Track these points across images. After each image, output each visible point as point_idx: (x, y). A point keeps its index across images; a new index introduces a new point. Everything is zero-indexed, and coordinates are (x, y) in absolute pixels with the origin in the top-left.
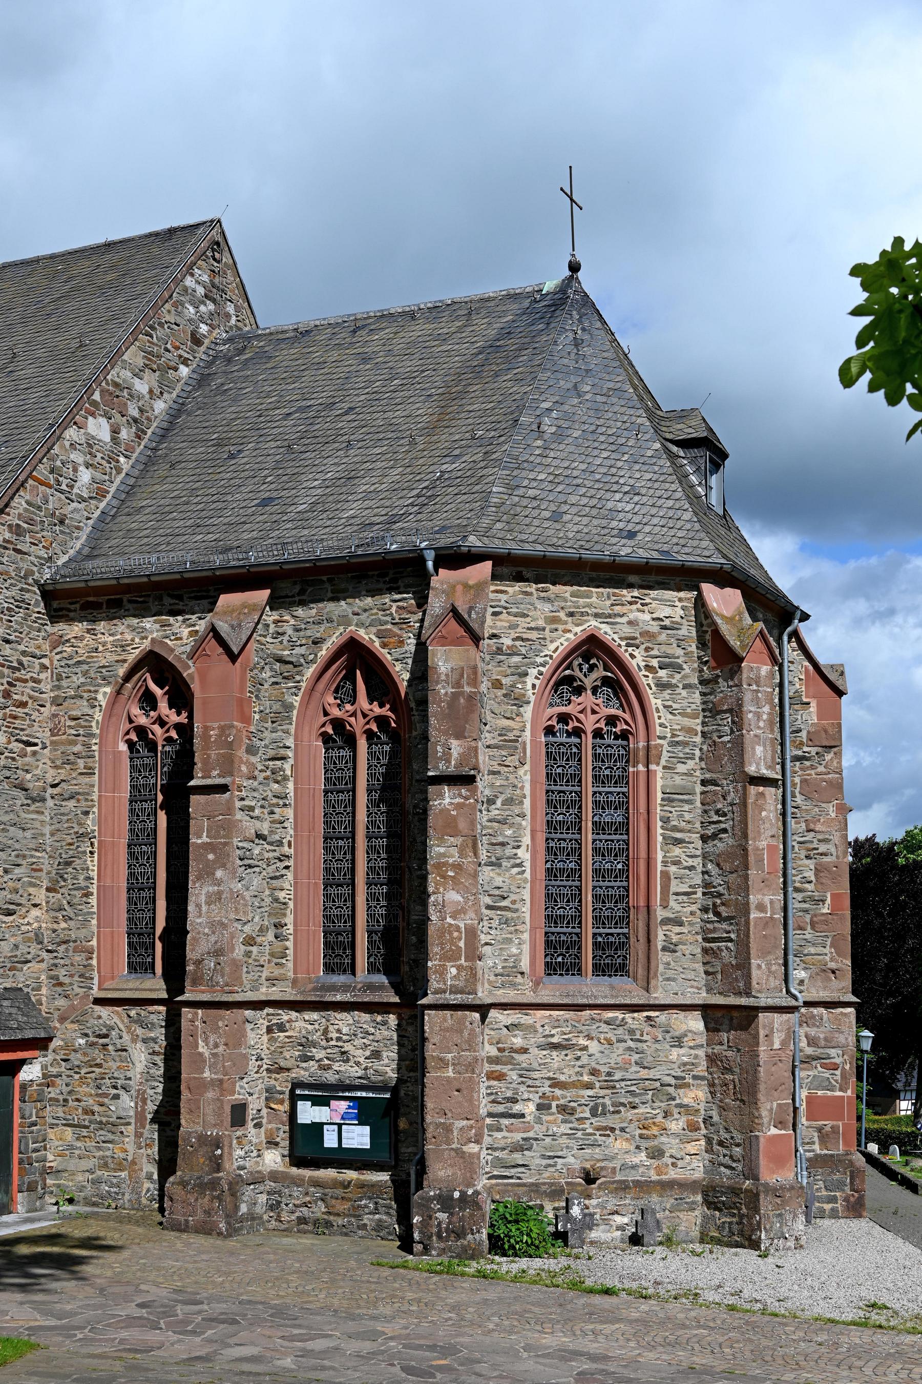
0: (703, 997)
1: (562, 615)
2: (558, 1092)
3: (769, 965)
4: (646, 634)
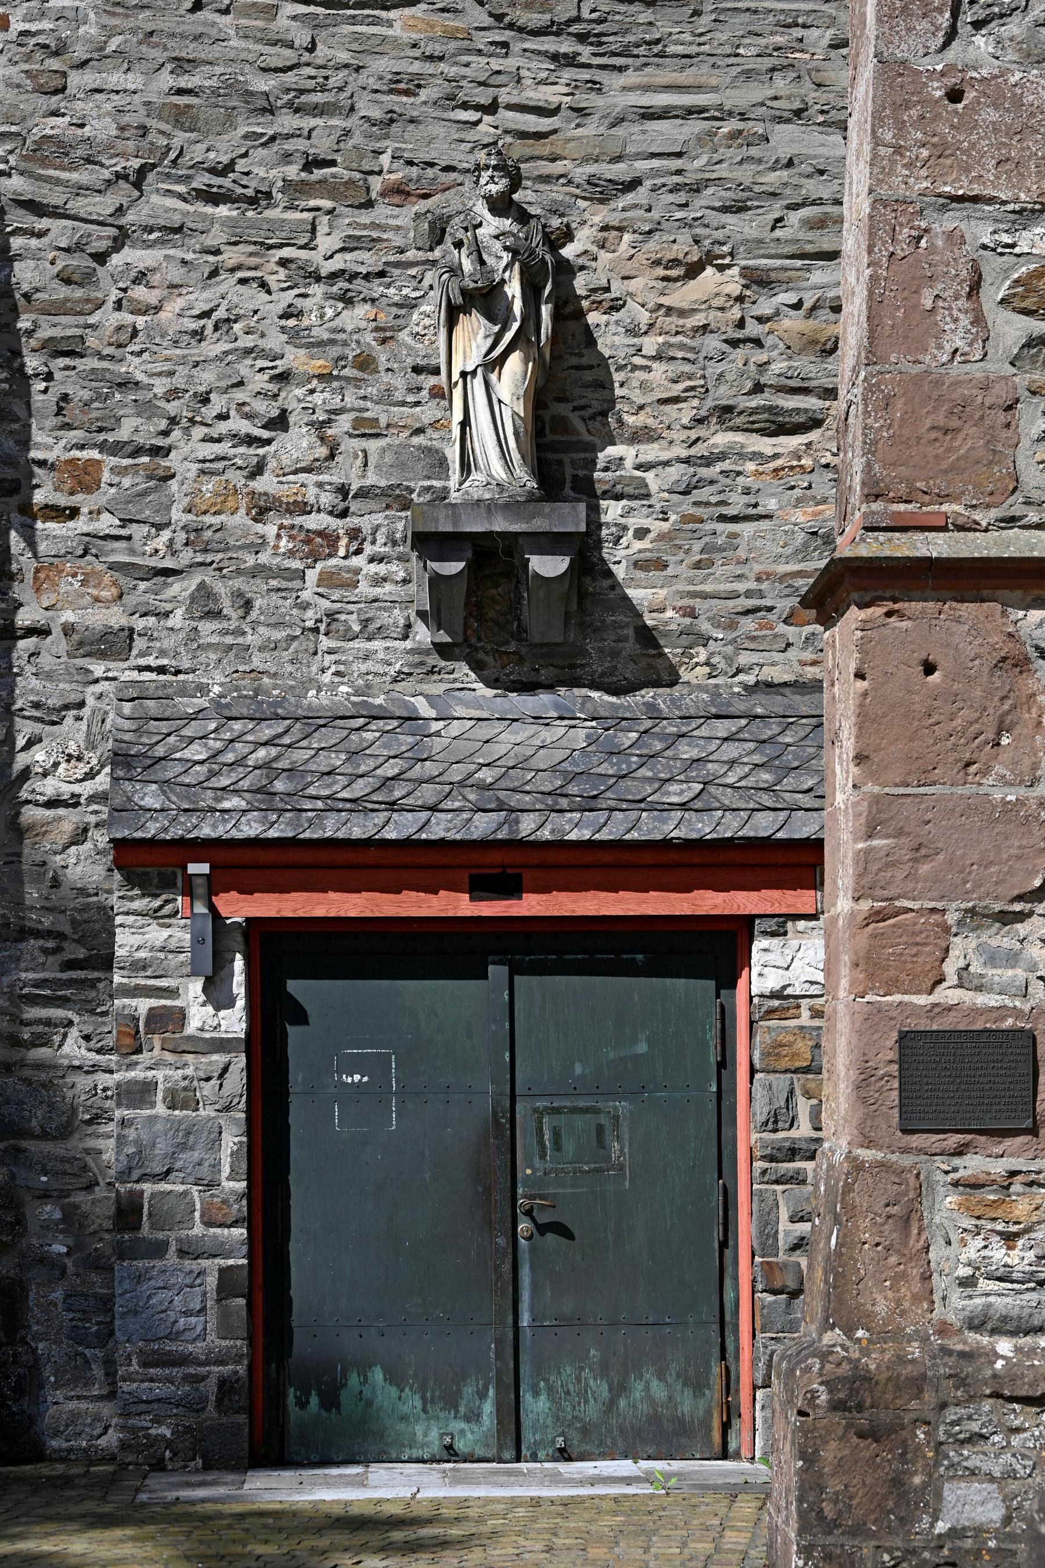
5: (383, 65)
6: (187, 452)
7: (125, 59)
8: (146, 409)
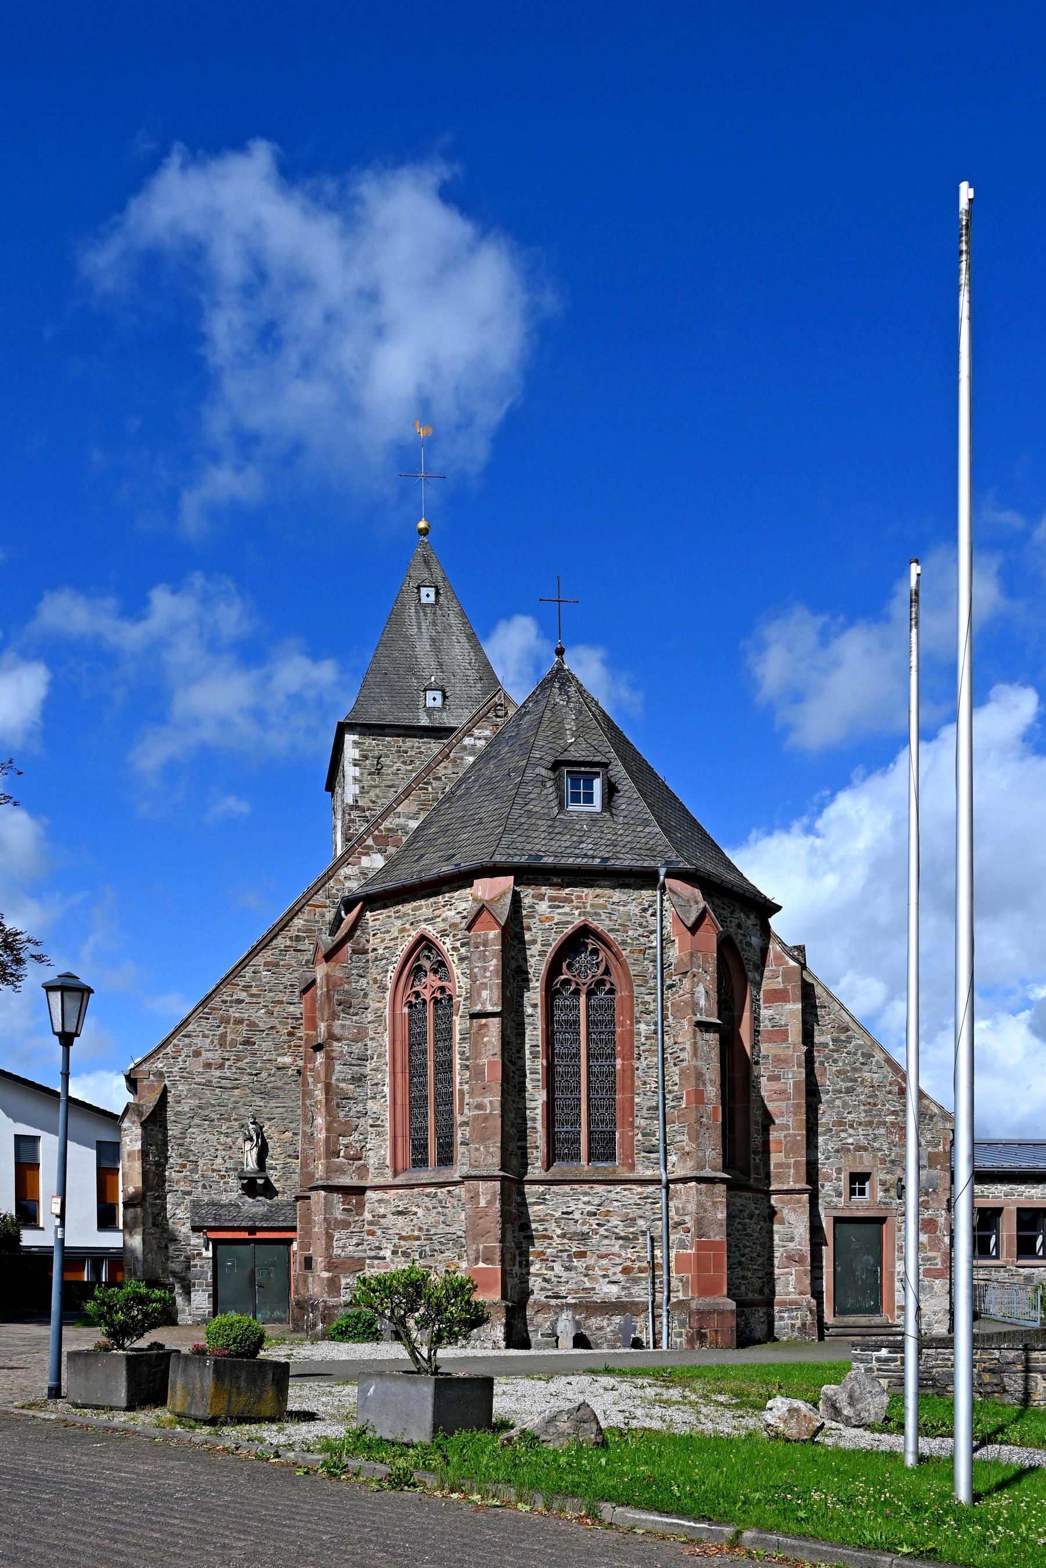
1: (407, 926)
2: (403, 1243)
3: (486, 1148)
4: (454, 926)
5: (233, 1099)
6: (201, 1162)
7: (190, 1098)
8: (195, 1155)
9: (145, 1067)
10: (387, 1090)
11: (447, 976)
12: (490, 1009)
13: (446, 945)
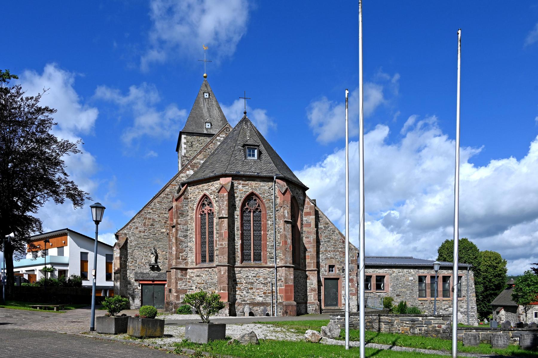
0: (227, 264)
4: (214, 191)
6: (138, 260)
9: (121, 232)
10: (194, 239)
11: (212, 206)
12: (224, 216)
13: (212, 197)
